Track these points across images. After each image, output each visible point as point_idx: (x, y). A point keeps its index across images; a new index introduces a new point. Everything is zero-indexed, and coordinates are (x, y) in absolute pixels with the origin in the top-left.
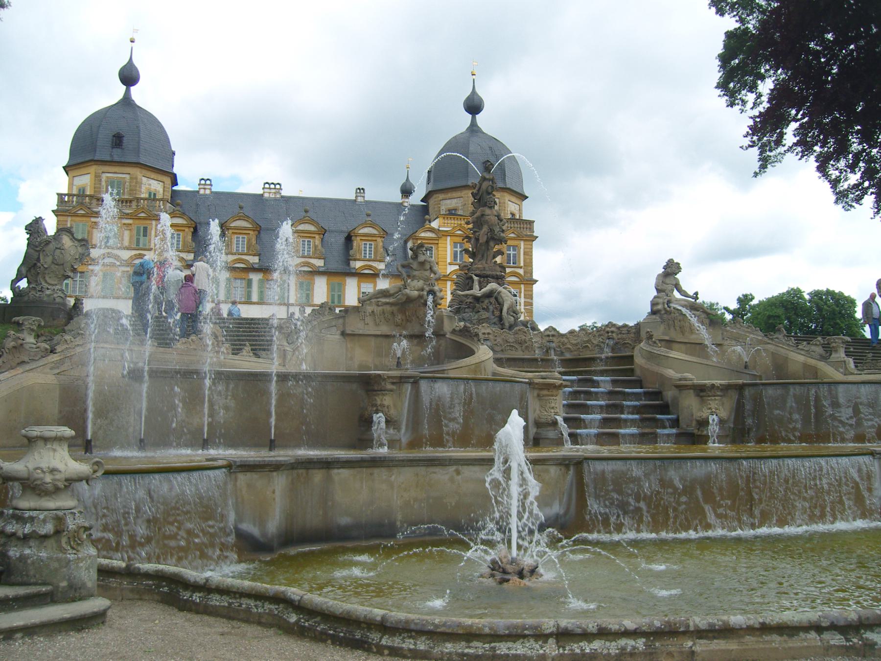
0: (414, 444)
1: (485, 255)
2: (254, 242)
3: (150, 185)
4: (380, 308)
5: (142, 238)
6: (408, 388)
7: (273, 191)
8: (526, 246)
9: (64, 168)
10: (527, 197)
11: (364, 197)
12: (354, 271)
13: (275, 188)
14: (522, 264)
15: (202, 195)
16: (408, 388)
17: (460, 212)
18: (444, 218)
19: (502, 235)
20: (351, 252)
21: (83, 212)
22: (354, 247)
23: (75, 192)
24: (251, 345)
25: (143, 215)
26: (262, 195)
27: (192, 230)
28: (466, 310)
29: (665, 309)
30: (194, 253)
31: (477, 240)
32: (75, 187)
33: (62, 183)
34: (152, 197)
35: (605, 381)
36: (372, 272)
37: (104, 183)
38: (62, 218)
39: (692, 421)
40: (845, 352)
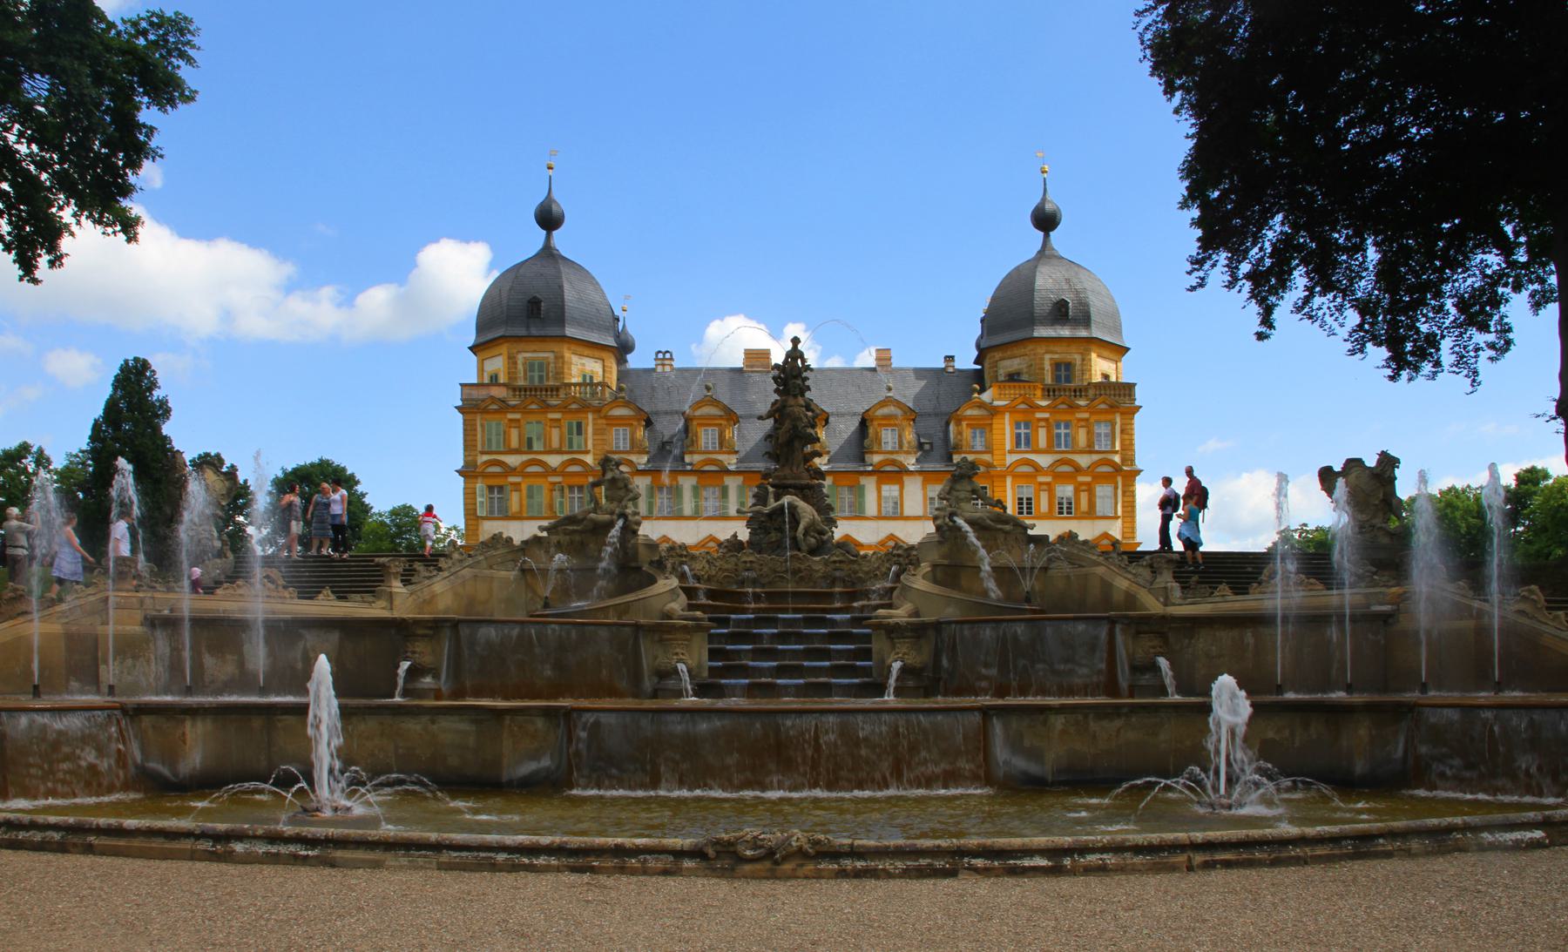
0: (458, 693)
3: (583, 365)
4: (568, 537)
5: (575, 438)
6: (447, 633)
8: (1124, 421)
9: (470, 348)
10: (1128, 349)
14: (1118, 448)
16: (447, 633)
17: (1025, 377)
18: (1000, 387)
20: (867, 442)
21: (495, 407)
23: (486, 381)
24: (331, 587)
25: (574, 406)
29: (946, 524)
31: (778, 438)
32: (485, 374)
33: (468, 369)
34: (588, 381)
36: (896, 469)
37: (520, 367)
38: (469, 417)
40: (1174, 572)
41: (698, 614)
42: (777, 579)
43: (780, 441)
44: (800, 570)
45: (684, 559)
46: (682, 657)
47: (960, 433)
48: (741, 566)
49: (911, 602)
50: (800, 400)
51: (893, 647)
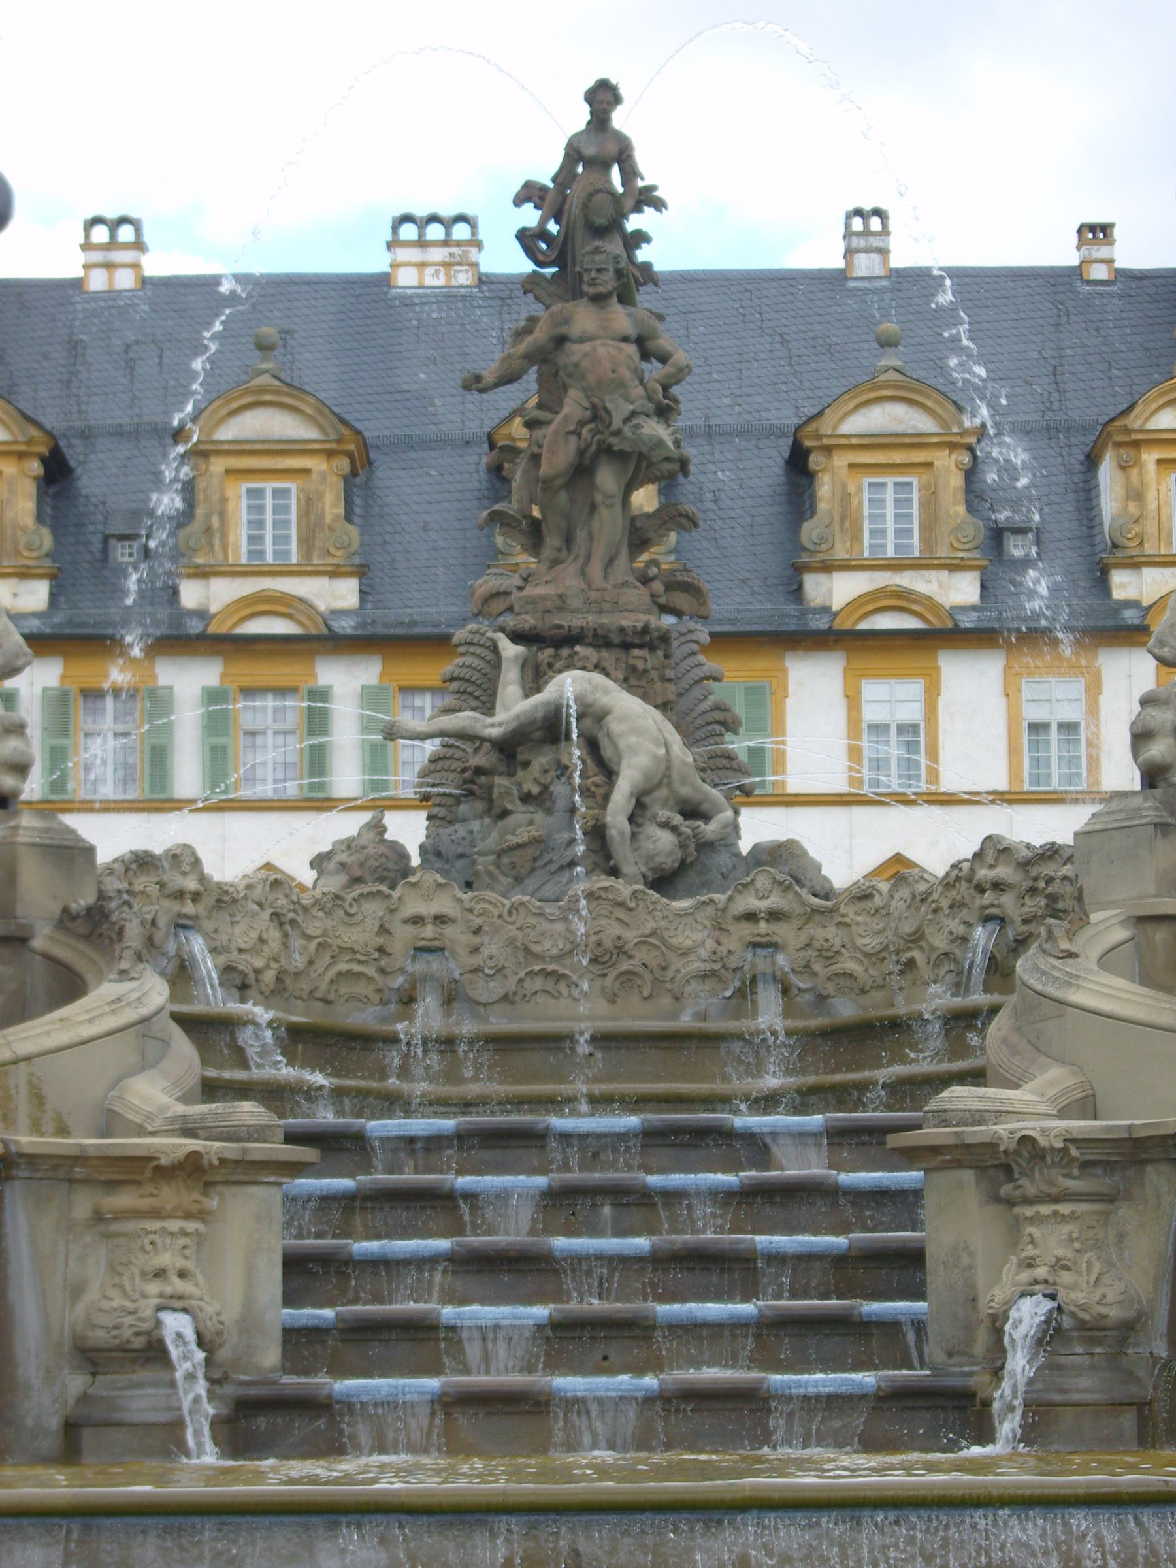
1: (581, 535)
2: (332, 506)
7: (437, 255)
11: (884, 252)
12: (821, 623)
13: (446, 243)
15: (96, 296)
19: (654, 429)
20: (809, 531)
22: (822, 506)
26: (383, 281)
27: (36, 467)
28: (464, 808)
30: (52, 577)
31: (536, 459)
35: (801, 1136)
39: (969, 1328)
41: (248, 1111)
42: (538, 984)
43: (544, 469)
44: (621, 950)
45: (189, 908)
46: (179, 1285)
47: (1136, 495)
48: (403, 935)
49: (1061, 1061)
50: (621, 318)
51: (1014, 1232)
